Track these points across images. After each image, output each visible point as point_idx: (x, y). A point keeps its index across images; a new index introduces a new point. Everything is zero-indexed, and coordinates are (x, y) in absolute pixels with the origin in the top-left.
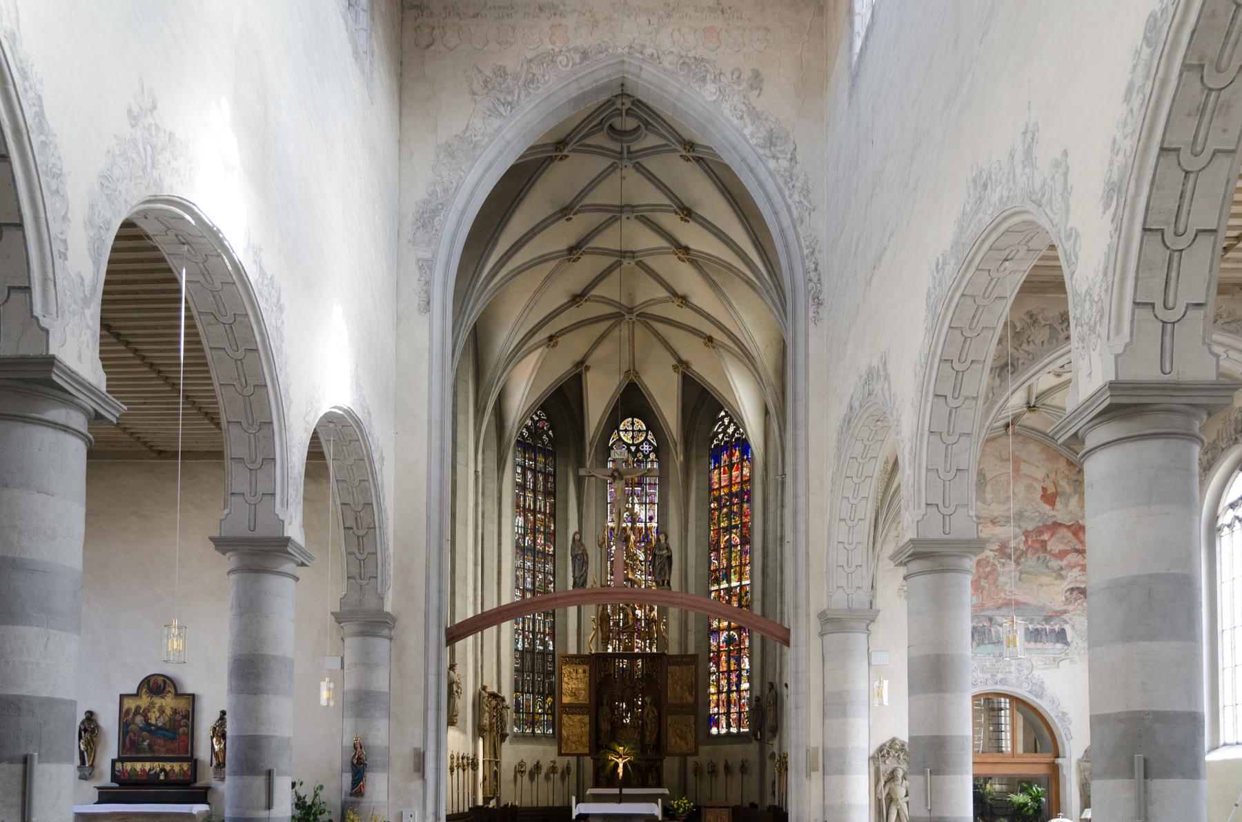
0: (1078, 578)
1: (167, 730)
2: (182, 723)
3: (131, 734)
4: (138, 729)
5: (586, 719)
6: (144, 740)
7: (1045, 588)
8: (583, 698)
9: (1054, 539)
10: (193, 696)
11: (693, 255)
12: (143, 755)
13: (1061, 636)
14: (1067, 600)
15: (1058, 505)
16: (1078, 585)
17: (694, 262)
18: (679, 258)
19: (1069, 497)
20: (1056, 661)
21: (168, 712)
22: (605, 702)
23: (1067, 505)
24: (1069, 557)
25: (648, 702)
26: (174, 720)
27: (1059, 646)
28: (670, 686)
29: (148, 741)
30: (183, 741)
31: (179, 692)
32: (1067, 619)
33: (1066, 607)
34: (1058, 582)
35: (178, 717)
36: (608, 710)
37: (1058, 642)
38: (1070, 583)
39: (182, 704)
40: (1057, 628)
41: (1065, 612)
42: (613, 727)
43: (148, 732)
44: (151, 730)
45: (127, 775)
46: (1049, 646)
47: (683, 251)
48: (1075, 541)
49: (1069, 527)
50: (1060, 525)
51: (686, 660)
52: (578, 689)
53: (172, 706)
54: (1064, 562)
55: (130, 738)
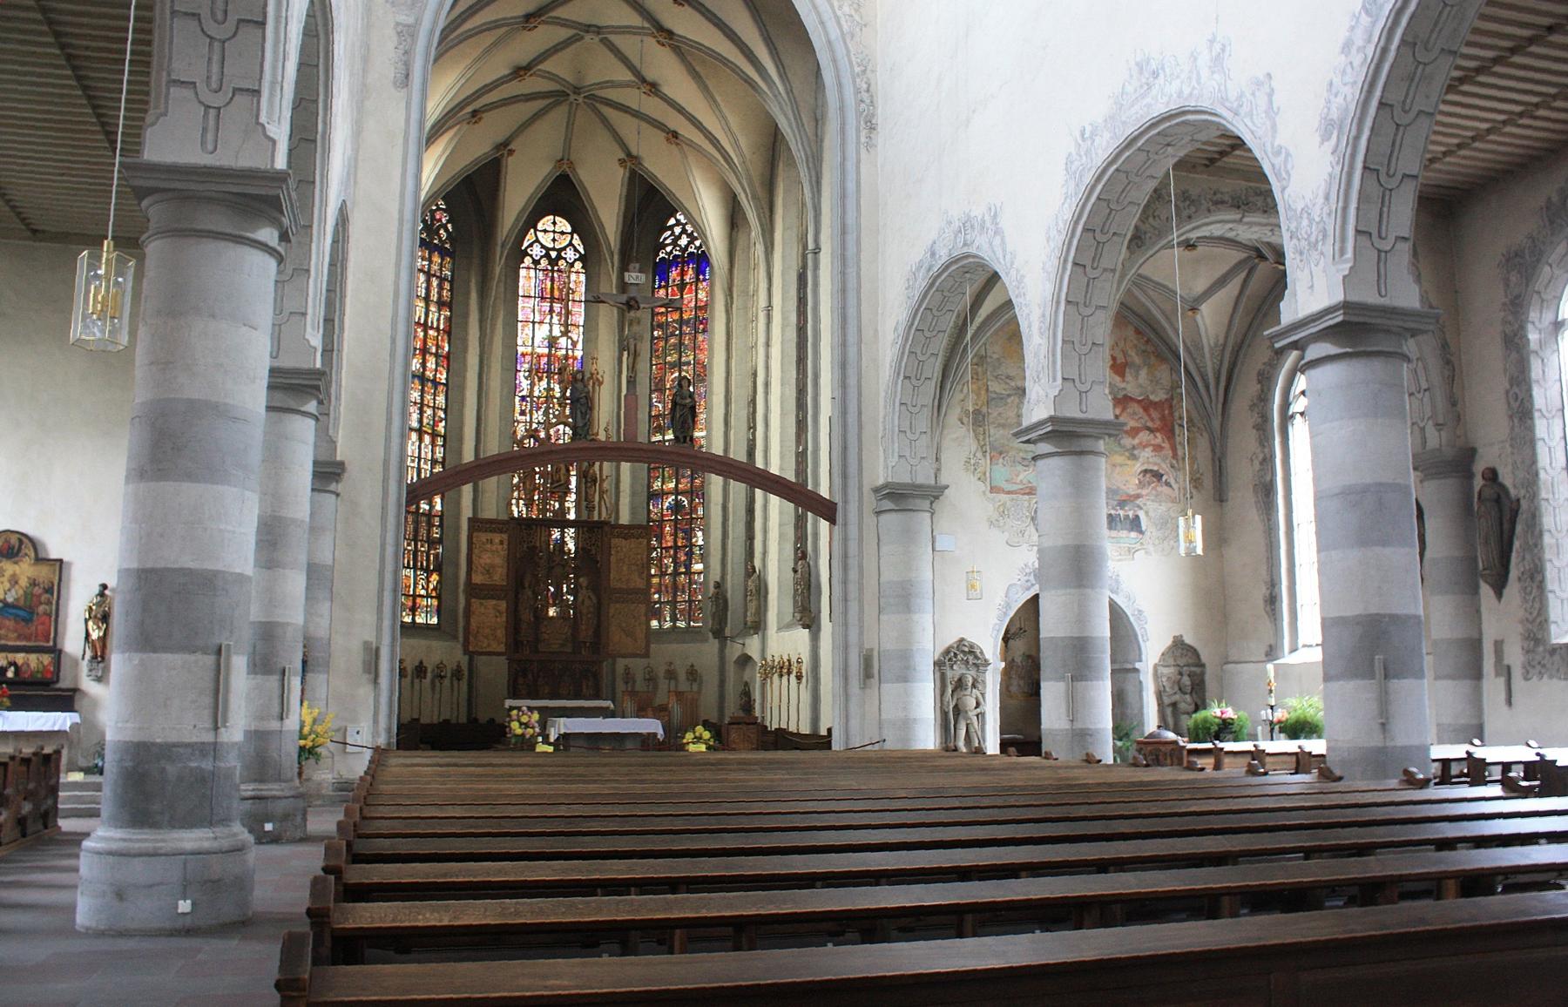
0: (1151, 460)
5: (503, 605)
7: (1118, 469)
8: (499, 577)
9: (1125, 414)
11: (678, 41)
13: (1135, 524)
14: (1140, 482)
15: (1129, 377)
16: (1151, 467)
17: (677, 50)
18: (658, 42)
19: (1139, 368)
20: (1131, 552)
21: (24, 582)
22: (527, 585)
23: (1137, 378)
24: (1141, 434)
25: (584, 585)
26: (32, 595)
27: (1133, 534)
28: (613, 566)
31: (40, 556)
32: (1141, 504)
33: (1139, 491)
34: (1129, 462)
36: (530, 593)
37: (1132, 530)
38: (1143, 464)
39: (43, 573)
40: (1131, 514)
41: (1138, 496)
42: (536, 617)
46: (1124, 533)
47: (666, 35)
48: (1147, 418)
49: (1139, 402)
50: (1131, 399)
51: (645, 530)
52: (493, 566)
54: (1136, 441)
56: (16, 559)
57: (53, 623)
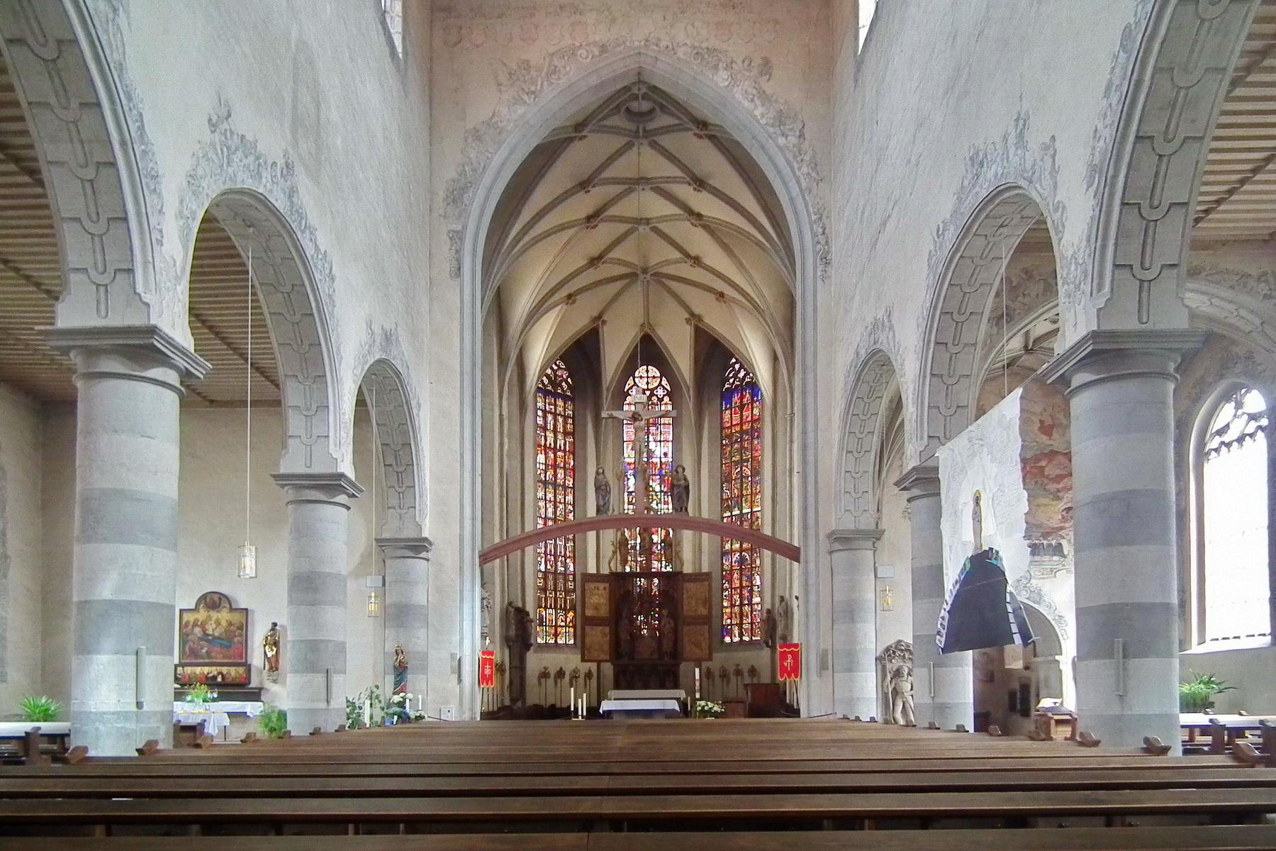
1: (222, 639)
6: (202, 648)
10: (246, 609)
12: (202, 661)
21: (224, 623)
29: (206, 649)
35: (232, 628)
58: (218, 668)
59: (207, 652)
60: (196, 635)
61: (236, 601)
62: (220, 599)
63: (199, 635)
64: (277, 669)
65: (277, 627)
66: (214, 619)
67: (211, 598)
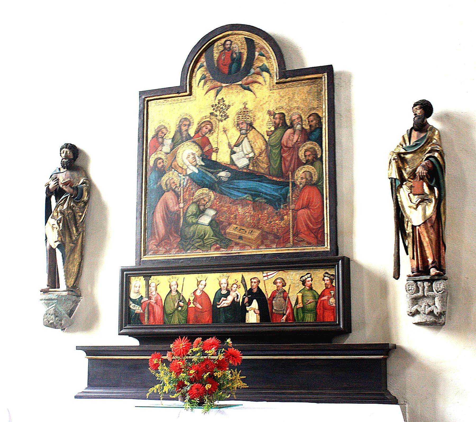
1: (260, 178)
2: (301, 154)
3: (169, 196)
4: (184, 181)
6: (201, 212)
10: (329, 69)
26: (281, 146)
29: (212, 213)
30: (307, 206)
43: (211, 187)
44: (220, 181)
45: (158, 310)
53: (272, 108)
55: (167, 207)
56: (244, 80)
57: (326, 202)
58: (248, 276)
59: (214, 223)
60: (181, 170)
61: (296, 52)
62: (250, 43)
63: (193, 169)
64: (441, 276)
65: (431, 121)
66: (232, 113)
67: (227, 49)
